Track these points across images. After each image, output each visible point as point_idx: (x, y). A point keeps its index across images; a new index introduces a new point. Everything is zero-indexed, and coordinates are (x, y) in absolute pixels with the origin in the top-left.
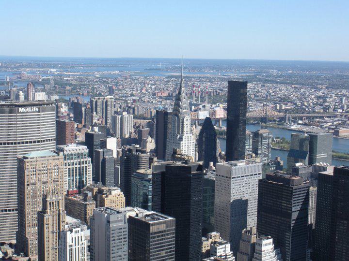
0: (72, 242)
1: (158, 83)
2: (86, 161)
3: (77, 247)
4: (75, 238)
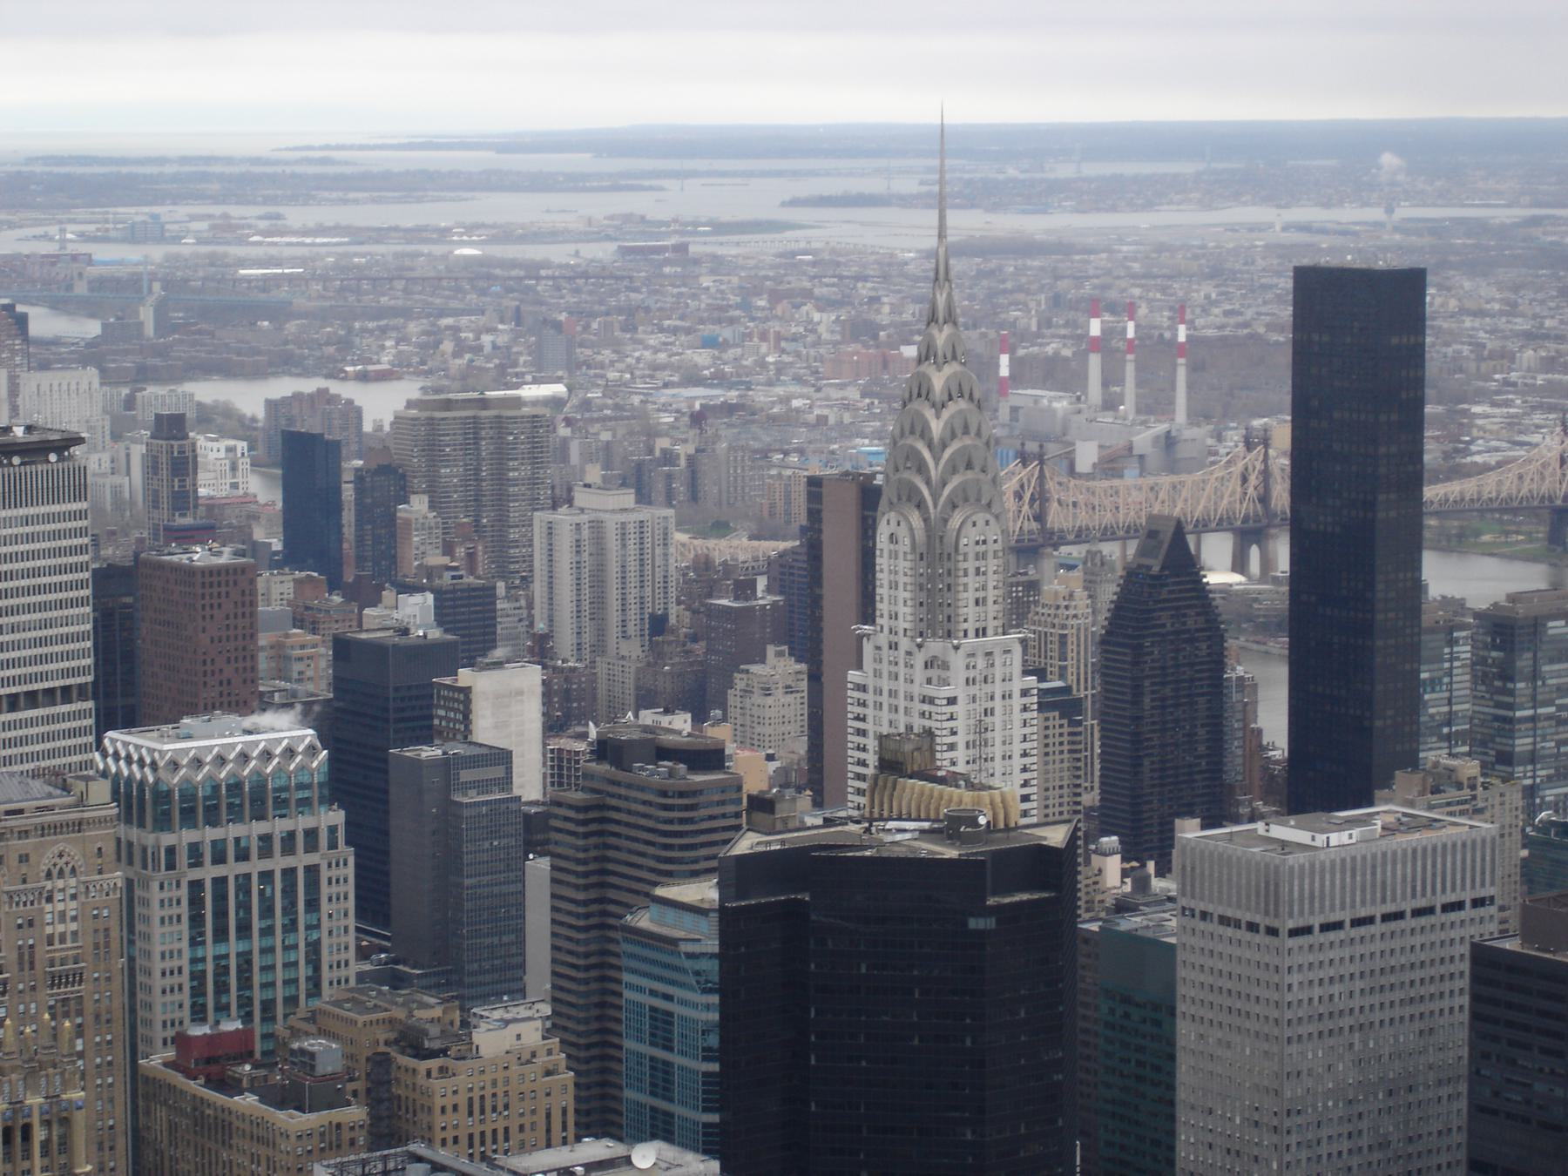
1: (864, 289)
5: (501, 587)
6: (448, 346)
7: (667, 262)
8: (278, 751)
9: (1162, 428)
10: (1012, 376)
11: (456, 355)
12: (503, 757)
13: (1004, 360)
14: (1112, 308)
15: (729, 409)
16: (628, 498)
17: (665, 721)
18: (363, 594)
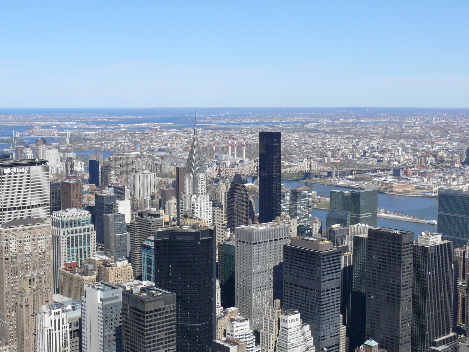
0: (51, 326)
2: (88, 229)
3: (57, 331)
4: (55, 321)
5: (126, 187)
6: (119, 145)
7: (158, 131)
8: (83, 214)
9: (241, 159)
10: (216, 150)
11: (121, 147)
12: (123, 216)
13: (214, 147)
14: (233, 139)
15: (168, 156)
16: (147, 171)
17: (152, 209)
18: (102, 188)
